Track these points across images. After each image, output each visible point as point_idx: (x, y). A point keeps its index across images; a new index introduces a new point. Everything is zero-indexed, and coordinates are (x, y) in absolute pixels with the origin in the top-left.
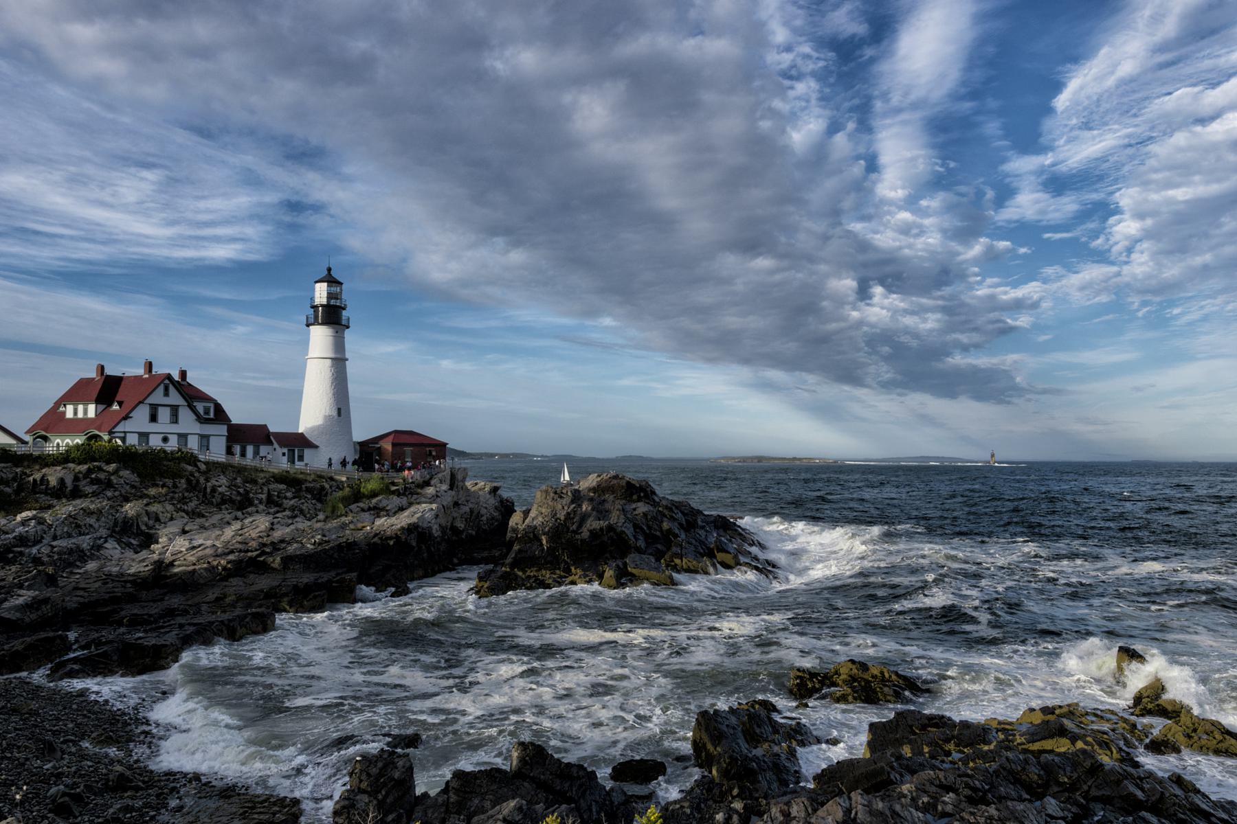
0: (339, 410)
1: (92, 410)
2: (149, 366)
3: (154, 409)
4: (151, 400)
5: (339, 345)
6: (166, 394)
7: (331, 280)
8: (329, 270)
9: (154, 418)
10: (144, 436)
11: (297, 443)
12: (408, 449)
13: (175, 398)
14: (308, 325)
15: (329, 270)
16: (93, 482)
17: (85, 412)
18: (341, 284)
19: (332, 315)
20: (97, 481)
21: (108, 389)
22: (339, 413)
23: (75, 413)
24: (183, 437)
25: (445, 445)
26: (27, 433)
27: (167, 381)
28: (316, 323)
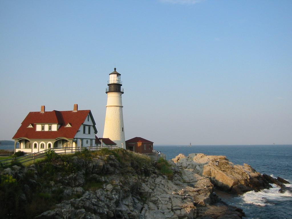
0: (123, 128)
1: (55, 128)
2: (76, 106)
3: (85, 126)
4: (85, 123)
5: (121, 101)
6: (88, 120)
7: (115, 73)
8: (115, 69)
9: (84, 132)
10: (82, 139)
11: (108, 141)
12: (145, 145)
13: (90, 123)
14: (107, 93)
15: (115, 69)
16: (111, 165)
17: (50, 128)
18: (120, 75)
19: (116, 88)
20: (111, 165)
21: (59, 117)
22: (123, 131)
23: (43, 128)
24: (91, 140)
25: (152, 143)
26: (13, 138)
27: (89, 114)
28: (110, 92)
